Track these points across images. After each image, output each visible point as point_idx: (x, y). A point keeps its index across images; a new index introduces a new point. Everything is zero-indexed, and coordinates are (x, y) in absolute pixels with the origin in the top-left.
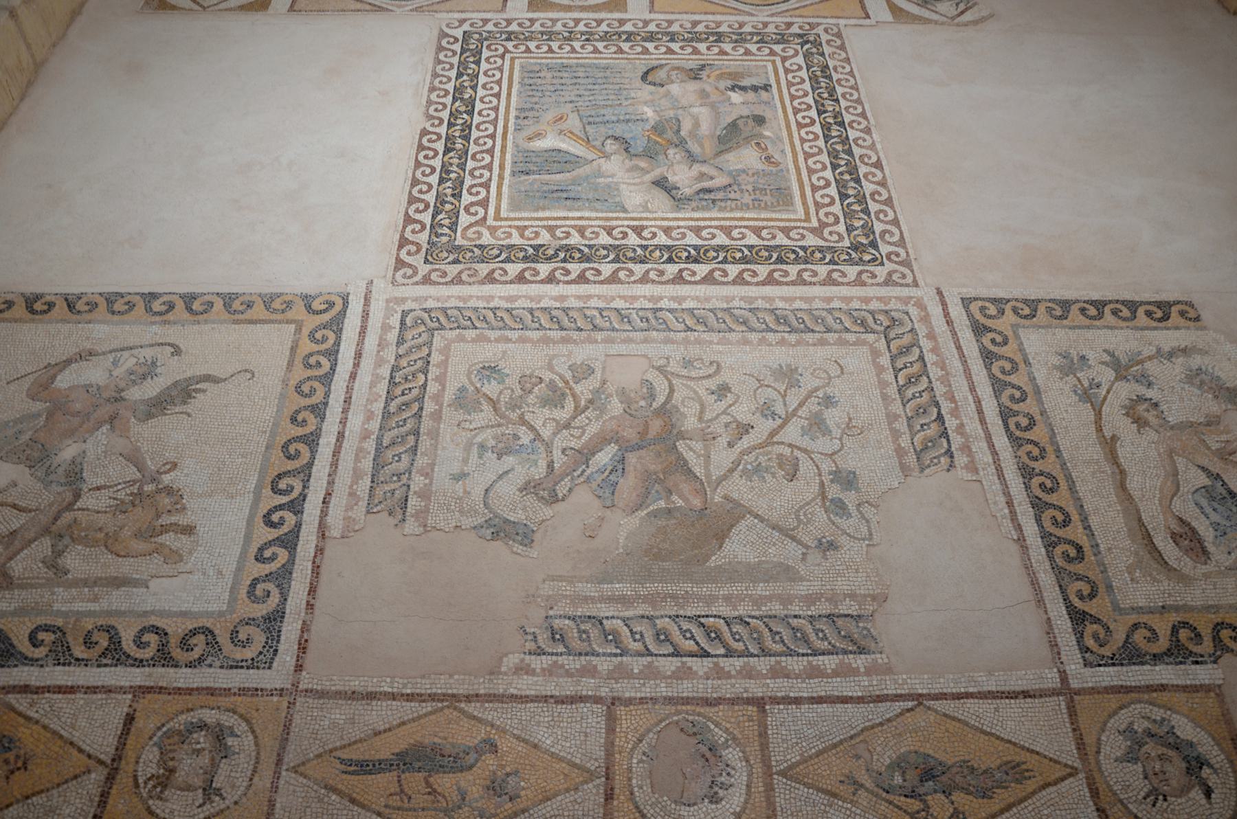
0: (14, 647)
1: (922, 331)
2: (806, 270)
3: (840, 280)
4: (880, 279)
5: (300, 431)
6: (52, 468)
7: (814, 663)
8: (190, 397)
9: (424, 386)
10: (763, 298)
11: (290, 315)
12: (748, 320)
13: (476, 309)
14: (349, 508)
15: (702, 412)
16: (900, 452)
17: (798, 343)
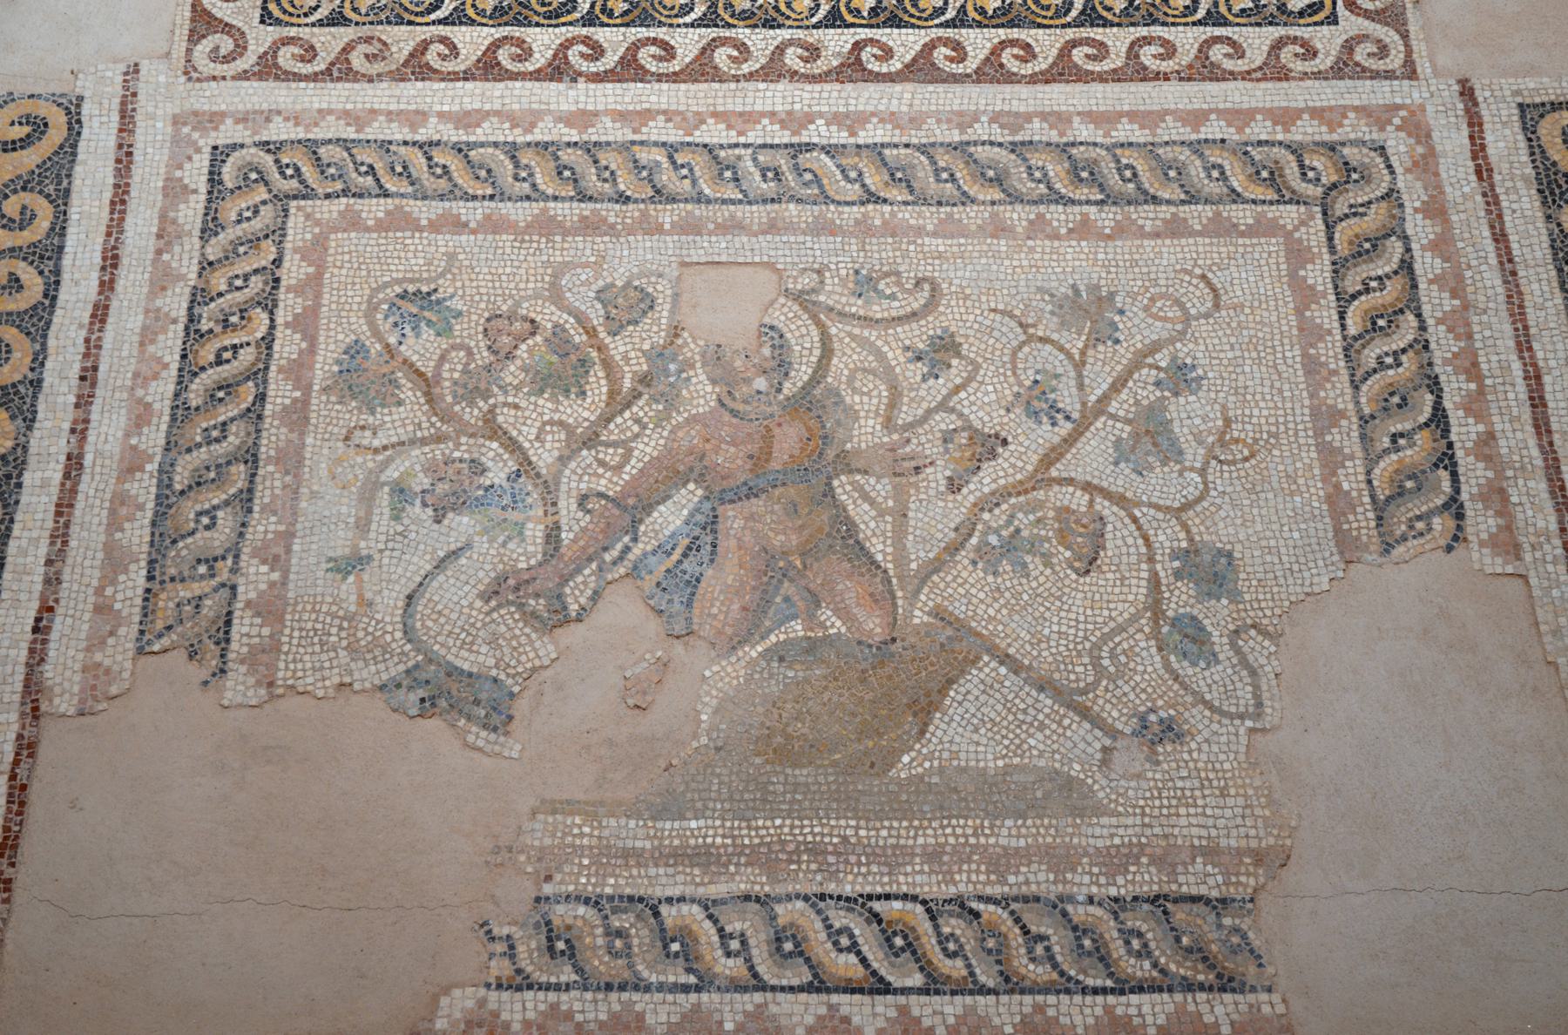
1: (1413, 194)
2: (1147, 41)
3: (1228, 65)
4: (1324, 62)
7: (1119, 1011)
9: (268, 341)
10: (1044, 116)
12: (1006, 172)
13: (385, 146)
14: (96, 642)
15: (893, 404)
16: (1337, 502)
17: (1120, 231)
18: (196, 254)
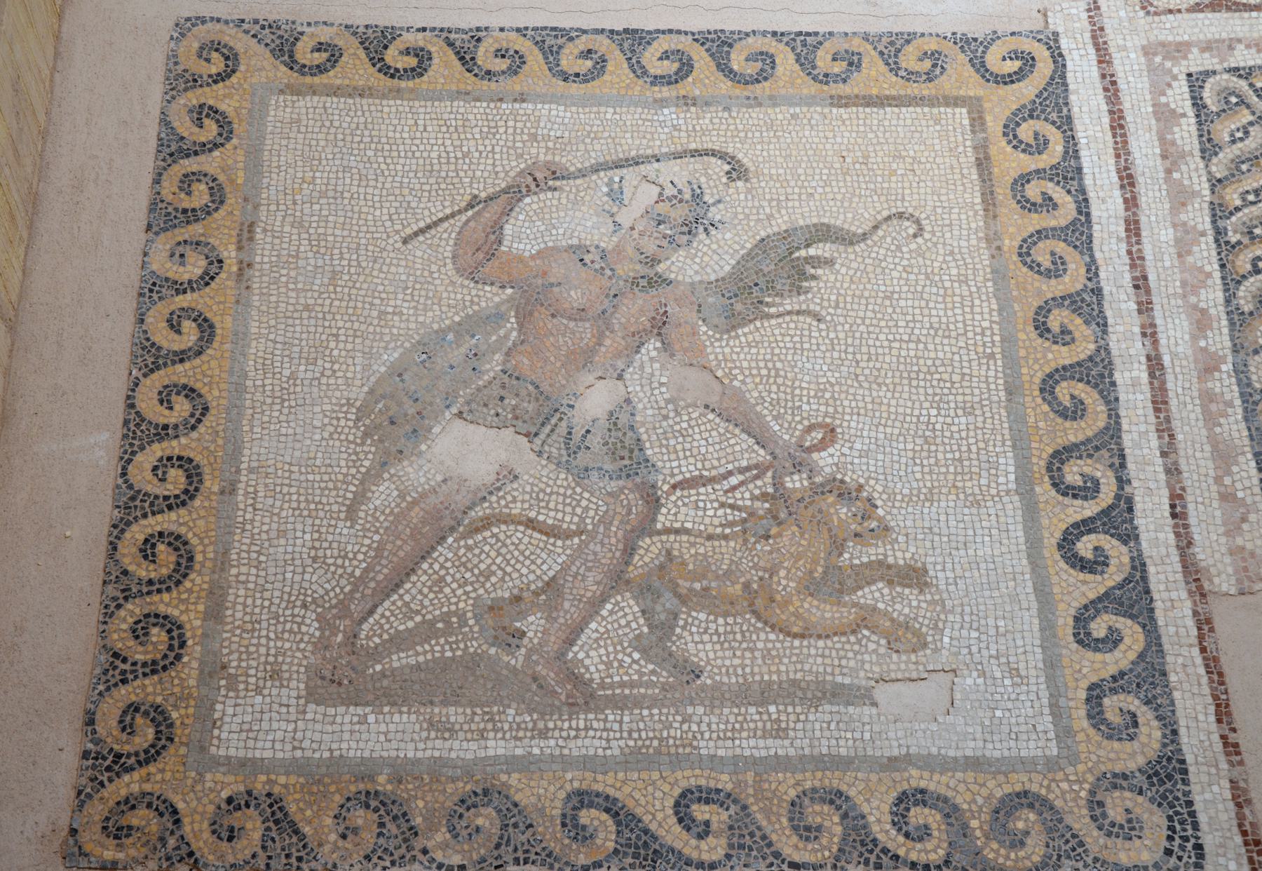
0: (655, 838)
5: (1065, 356)
6: (577, 436)
8: (803, 275)
11: (946, 84)
18: (1203, 172)
